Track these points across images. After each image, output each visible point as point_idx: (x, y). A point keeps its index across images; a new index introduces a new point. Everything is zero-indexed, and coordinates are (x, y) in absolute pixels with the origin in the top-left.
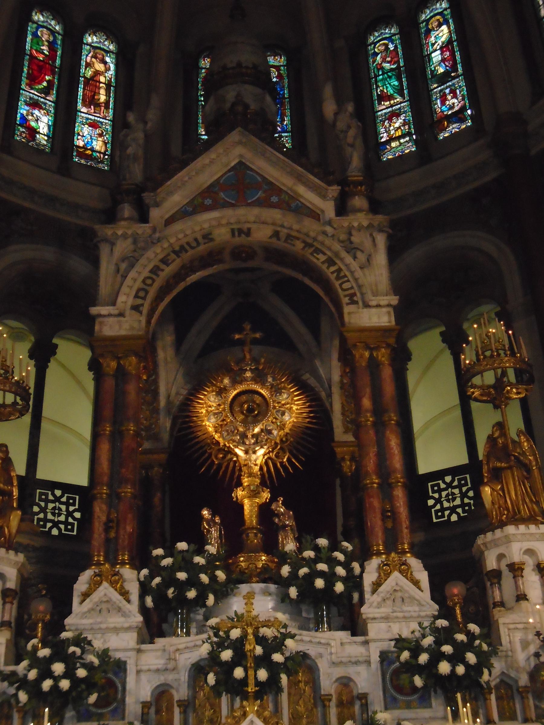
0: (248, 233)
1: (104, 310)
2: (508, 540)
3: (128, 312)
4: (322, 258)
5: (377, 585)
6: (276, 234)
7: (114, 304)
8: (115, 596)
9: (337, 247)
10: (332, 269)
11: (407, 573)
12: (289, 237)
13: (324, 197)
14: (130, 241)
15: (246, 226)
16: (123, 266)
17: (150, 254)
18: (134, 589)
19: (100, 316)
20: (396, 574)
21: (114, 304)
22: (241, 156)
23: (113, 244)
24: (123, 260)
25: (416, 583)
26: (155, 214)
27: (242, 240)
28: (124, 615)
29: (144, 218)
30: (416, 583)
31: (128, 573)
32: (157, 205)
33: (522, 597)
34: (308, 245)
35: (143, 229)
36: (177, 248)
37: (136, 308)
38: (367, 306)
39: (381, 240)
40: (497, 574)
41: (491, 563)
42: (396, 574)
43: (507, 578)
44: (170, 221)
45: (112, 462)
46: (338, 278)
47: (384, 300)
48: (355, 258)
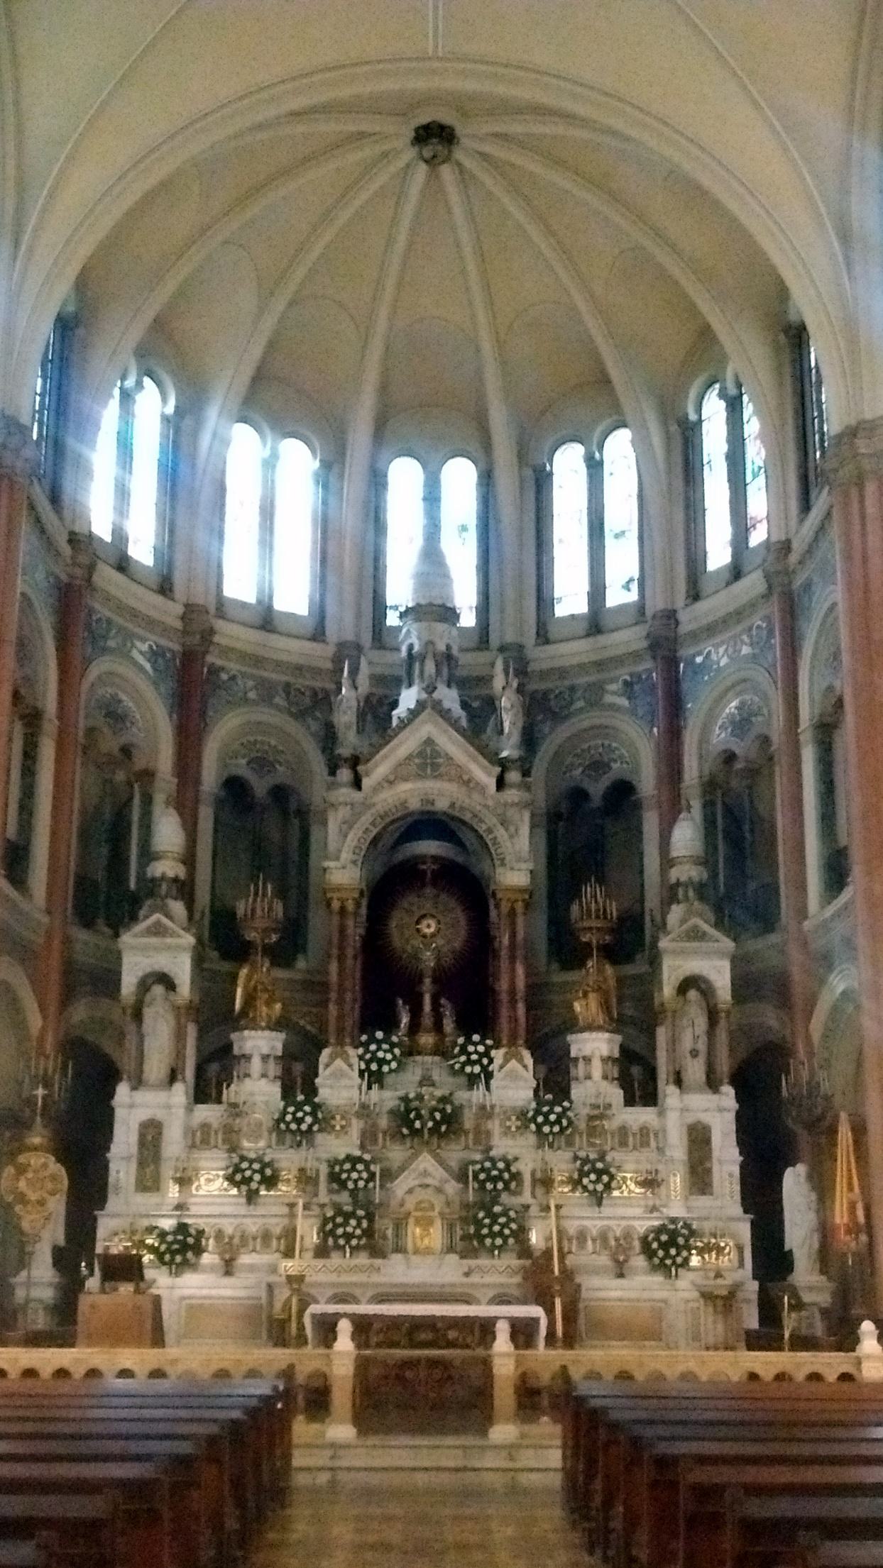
0: (433, 804)
1: (330, 864)
2: (585, 1041)
3: (350, 866)
4: (484, 827)
5: (501, 1067)
6: (453, 805)
7: (337, 859)
8: (345, 1067)
9: (495, 820)
10: (490, 836)
11: (521, 1060)
12: (462, 808)
13: (489, 774)
14: (349, 807)
15: (431, 797)
16: (345, 827)
17: (363, 818)
18: (355, 1061)
19: (328, 868)
20: (514, 1061)
21: (337, 859)
22: (429, 733)
23: (336, 810)
24: (344, 823)
25: (525, 1067)
26: (366, 782)
27: (429, 808)
28: (350, 1078)
29: (357, 784)
30: (525, 1067)
31: (353, 1053)
32: (367, 775)
33: (588, 1077)
34: (475, 816)
35: (357, 796)
36: (382, 813)
37: (354, 862)
38: (512, 869)
39: (527, 816)
40: (576, 1060)
41: (573, 1054)
42: (514, 1061)
43: (581, 1064)
44: (377, 788)
45: (340, 974)
46: (494, 844)
47: (524, 866)
48: (507, 830)
